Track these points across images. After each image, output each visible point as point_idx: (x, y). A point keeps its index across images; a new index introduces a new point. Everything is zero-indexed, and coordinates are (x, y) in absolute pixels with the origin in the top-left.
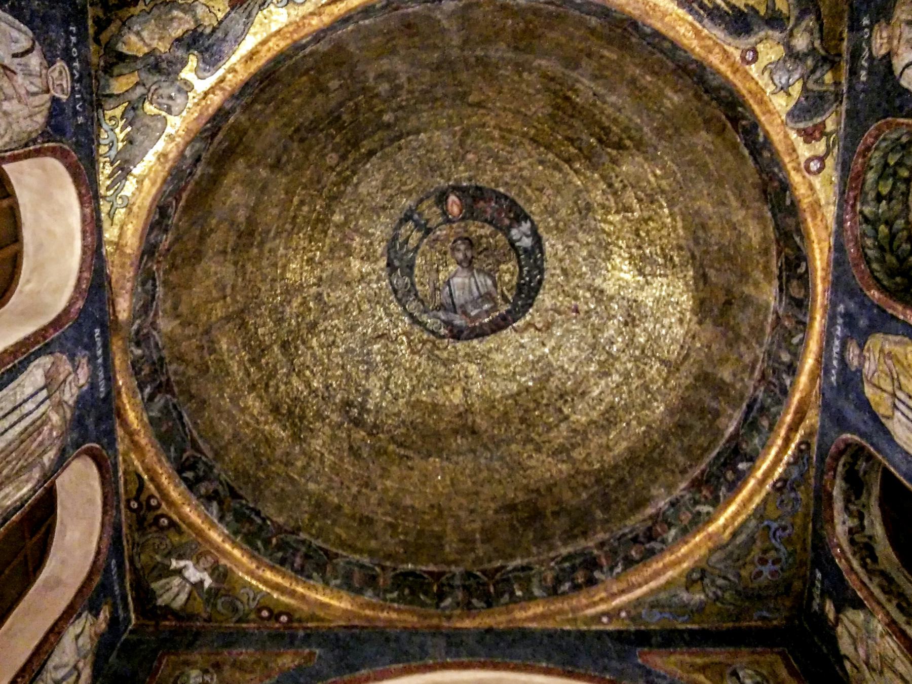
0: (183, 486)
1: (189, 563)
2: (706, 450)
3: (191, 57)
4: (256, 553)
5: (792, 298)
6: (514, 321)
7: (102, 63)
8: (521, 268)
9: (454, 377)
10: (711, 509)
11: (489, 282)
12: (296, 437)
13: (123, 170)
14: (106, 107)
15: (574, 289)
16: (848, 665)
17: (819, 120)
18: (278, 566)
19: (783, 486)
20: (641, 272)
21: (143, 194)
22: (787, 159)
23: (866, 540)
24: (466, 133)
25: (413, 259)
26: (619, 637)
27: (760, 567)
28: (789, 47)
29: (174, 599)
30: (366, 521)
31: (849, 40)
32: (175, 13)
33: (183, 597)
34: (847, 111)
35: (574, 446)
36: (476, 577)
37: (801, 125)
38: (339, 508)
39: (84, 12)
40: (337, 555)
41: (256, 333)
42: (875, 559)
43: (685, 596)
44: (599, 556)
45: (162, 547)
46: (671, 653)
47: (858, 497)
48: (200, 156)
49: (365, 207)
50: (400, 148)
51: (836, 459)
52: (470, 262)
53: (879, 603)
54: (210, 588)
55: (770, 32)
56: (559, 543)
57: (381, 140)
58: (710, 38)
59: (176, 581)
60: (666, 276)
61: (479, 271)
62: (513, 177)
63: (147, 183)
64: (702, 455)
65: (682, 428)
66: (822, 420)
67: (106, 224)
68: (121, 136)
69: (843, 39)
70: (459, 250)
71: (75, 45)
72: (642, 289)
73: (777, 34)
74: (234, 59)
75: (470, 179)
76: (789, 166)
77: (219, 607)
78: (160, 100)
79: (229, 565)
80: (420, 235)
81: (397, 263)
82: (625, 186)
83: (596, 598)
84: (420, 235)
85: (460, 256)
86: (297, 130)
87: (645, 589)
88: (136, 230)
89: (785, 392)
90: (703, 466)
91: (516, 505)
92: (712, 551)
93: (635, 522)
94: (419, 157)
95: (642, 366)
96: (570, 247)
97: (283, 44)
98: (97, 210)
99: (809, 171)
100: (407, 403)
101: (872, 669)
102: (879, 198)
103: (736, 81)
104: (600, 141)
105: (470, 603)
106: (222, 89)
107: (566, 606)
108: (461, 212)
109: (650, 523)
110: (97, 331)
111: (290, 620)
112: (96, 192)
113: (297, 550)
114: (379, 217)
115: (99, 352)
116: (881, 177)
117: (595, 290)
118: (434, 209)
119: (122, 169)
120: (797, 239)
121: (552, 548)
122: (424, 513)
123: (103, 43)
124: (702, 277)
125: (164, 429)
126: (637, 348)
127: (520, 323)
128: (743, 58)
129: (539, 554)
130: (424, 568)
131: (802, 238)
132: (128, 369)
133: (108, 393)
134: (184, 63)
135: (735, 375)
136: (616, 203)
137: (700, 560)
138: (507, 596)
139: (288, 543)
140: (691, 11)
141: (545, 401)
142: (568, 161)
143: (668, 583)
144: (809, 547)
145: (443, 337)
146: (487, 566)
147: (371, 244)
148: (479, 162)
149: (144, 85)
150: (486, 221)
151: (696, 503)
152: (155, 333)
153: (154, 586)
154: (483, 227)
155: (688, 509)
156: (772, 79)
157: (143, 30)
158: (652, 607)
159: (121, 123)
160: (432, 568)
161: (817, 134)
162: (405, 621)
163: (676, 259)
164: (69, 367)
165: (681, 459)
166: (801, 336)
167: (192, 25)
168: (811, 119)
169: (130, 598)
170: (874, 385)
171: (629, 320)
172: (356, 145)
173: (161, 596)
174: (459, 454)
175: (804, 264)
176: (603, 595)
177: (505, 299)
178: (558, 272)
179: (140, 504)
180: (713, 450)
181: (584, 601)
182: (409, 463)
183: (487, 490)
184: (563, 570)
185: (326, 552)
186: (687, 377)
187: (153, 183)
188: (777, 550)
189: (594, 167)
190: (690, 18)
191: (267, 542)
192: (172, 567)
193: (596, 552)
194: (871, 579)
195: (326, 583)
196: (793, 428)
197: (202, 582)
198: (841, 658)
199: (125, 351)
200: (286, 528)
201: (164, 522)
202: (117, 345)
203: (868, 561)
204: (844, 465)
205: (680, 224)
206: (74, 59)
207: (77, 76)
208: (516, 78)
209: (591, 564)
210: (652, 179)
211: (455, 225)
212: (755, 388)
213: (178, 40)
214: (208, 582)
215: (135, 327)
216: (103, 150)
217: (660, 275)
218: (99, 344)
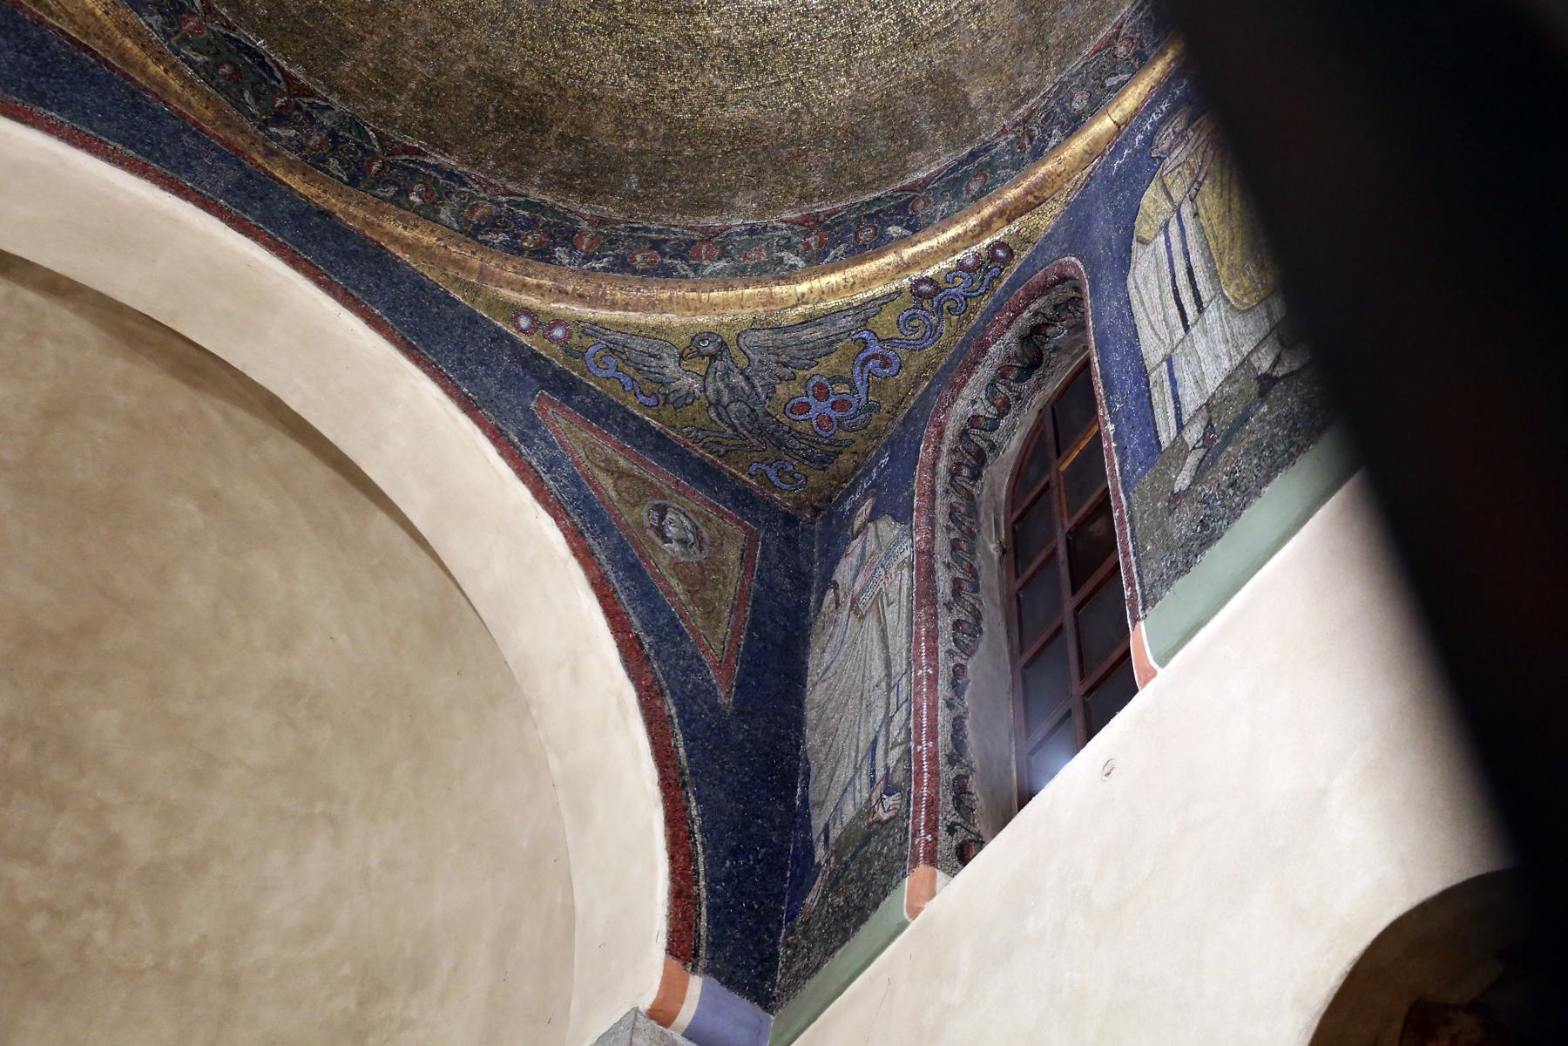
2: (861, 185)
10: (801, 264)
16: (830, 595)
19: (926, 293)
23: (985, 445)
26: (530, 360)
27: (811, 400)
35: (668, 64)
36: (362, 133)
42: (976, 476)
43: (671, 367)
44: (582, 234)
46: (589, 427)
47: (1019, 380)
51: (1031, 298)
53: (932, 522)
56: (537, 180)
64: (850, 189)
65: (855, 138)
66: (1058, 225)
83: (532, 281)
87: (617, 315)
89: (1038, 154)
91: (511, 85)
92: (756, 325)
93: (681, 224)
101: (854, 608)
105: (325, 161)
107: (476, 262)
109: (696, 236)
121: (520, 177)
129: (493, 173)
130: (284, 63)
135: (989, 98)
137: (730, 326)
138: (392, 190)
144: (901, 417)
146: (394, 134)
151: (788, 246)
155: (768, 247)
160: (297, 72)
162: (189, 105)
165: (818, 179)
166: (1126, 76)
170: (1164, 185)
176: (547, 282)
180: (873, 190)
181: (510, 273)
183: (479, 34)
184: (514, 218)
188: (853, 387)
193: (584, 225)
194: (947, 492)
196: (1008, 214)
198: (828, 582)
203: (965, 472)
204: (1036, 314)
212: (1004, 131)
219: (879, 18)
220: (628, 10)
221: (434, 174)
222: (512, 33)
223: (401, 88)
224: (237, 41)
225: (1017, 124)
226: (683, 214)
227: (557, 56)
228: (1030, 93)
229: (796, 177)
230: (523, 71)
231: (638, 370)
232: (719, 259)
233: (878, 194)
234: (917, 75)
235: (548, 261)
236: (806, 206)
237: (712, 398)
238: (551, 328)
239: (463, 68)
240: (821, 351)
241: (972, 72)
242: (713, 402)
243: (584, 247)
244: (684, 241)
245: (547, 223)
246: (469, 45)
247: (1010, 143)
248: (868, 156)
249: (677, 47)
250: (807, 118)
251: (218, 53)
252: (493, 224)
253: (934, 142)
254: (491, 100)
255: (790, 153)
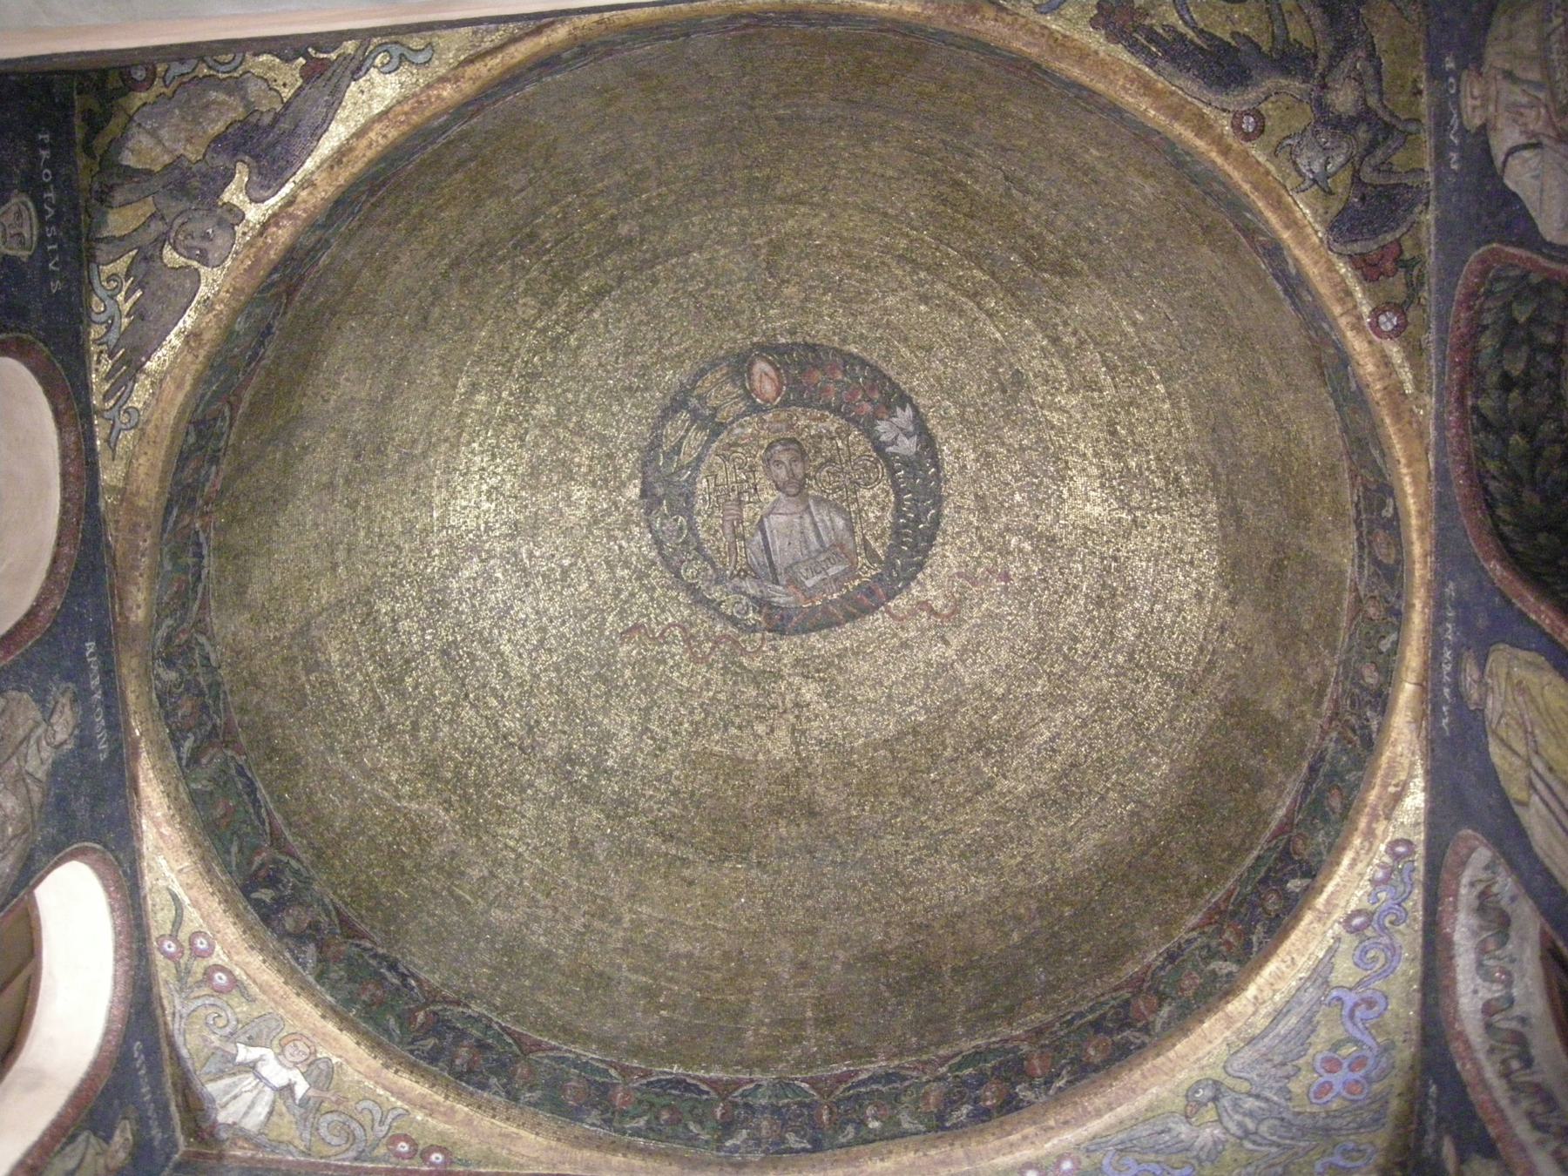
0: (253, 916)
1: (268, 1053)
2: (1237, 852)
3: (239, 166)
4: (384, 1039)
5: (1377, 563)
6: (889, 599)
7: (96, 186)
8: (898, 492)
9: (774, 707)
10: (1234, 968)
11: (840, 523)
12: (471, 827)
13: (130, 365)
14: (100, 259)
15: (1001, 535)
17: (1389, 238)
18: (423, 1064)
20: (1124, 503)
21: (161, 405)
22: (1337, 310)
24: (777, 248)
25: (692, 481)
28: (1321, 106)
29: (246, 1114)
30: (598, 982)
31: (1431, 94)
32: (213, 95)
33: (262, 1110)
34: (1437, 220)
35: (1000, 844)
36: (798, 1091)
37: (1357, 248)
38: (546, 956)
39: (67, 106)
40: (538, 1044)
41: (395, 631)
43: (1183, 1130)
44: (1027, 1057)
45: (221, 1023)
48: (269, 327)
49: (595, 388)
50: (655, 281)
52: (802, 486)
54: (305, 1101)
55: (1283, 82)
56: (960, 1030)
57: (615, 268)
58: (1172, 93)
59: (249, 1081)
60: (1168, 511)
61: (819, 501)
62: (875, 325)
63: (169, 384)
64: (1230, 861)
67: (103, 461)
68: (127, 307)
69: (1420, 92)
70: (779, 463)
71: (48, 164)
72: (1127, 535)
73: (1296, 85)
74: (310, 164)
75: (792, 332)
76: (1343, 322)
77: (323, 1131)
78: (189, 242)
79: (335, 1060)
80: (702, 436)
81: (660, 491)
82: (1082, 342)
84: (702, 436)
85: (782, 474)
86: (455, 264)
88: (153, 466)
90: (1229, 884)
91: (885, 954)
94: (691, 294)
95: (1131, 686)
96: (988, 455)
97: (393, 134)
98: (89, 437)
99: (1379, 333)
100: (684, 757)
102: (1507, 383)
103: (1229, 168)
104: (1028, 260)
105: (783, 1140)
106: (291, 217)
108: (778, 394)
109: (1125, 994)
110: (91, 646)
111: (449, 1160)
112: (88, 403)
113: (461, 1035)
114: (622, 404)
115: (95, 682)
116: (1506, 344)
117: (1040, 536)
118: (728, 387)
119: (128, 363)
120: (1376, 453)
122: (710, 968)
123: (98, 152)
124: (1232, 513)
125: (219, 811)
126: (1119, 650)
127: (900, 603)
128: (1237, 127)
130: (701, 1073)
131: (1383, 455)
132: (151, 706)
133: (116, 752)
134: (228, 177)
135: (1290, 706)
136: (1068, 372)
139: (445, 1022)
140: (1133, 47)
141: (949, 753)
142: (974, 296)
143: (1150, 1108)
145: (754, 629)
147: (610, 456)
148: (807, 299)
149: (163, 218)
150: (827, 406)
151: (1213, 955)
152: (202, 639)
153: (212, 1088)
154: (822, 419)
156: (1294, 163)
157: (161, 126)
158: (1122, 1150)
159: (127, 285)
160: (715, 1074)
161: (1389, 265)
163: (1185, 479)
164: (35, 713)
165: (1194, 869)
166: (1393, 637)
167: (239, 113)
168: (1375, 233)
169: (173, 1108)
171: (1105, 594)
172: (569, 281)
173: (224, 1106)
174: (782, 854)
175: (1390, 501)
177: (872, 555)
178: (970, 502)
179: (179, 945)
182: (686, 873)
185: (518, 1039)
186: (1209, 707)
187: (179, 387)
189: (1023, 308)
190: (1134, 62)
191: (405, 1019)
192: (239, 1059)
193: (1025, 1048)
195: (513, 1096)
197: (290, 1088)
199: (146, 674)
200: (446, 992)
201: (220, 979)
202: (129, 666)
205: (1187, 415)
206: (45, 187)
207: (51, 212)
208: (858, 150)
209: (1014, 1069)
210: (1131, 330)
211: (768, 417)
212: (1324, 733)
213: (219, 138)
214: (301, 1088)
215: (163, 632)
216: (95, 332)
217: (1158, 510)
218: (95, 668)
219: (1146, 688)
220: (938, 820)
221: (874, 1087)
222: (858, 907)
223: (802, 1023)
224: (659, 1081)
225: (1331, 720)
226: (1101, 977)
227: (906, 901)
228: (1322, 685)
229: (1174, 877)
230: (886, 934)
231: (1157, 1152)
232: (1160, 1006)
233: (1255, 853)
234: (1213, 716)
235: (1018, 1108)
236: (1201, 902)
237: (1239, 1133)
238: (1058, 1165)
239: (838, 967)
240: (1304, 1034)
241: (1258, 690)
242: (1239, 1133)
243: (1039, 1072)
244: (1120, 1006)
245: (994, 1068)
246: (831, 944)
247: (1337, 741)
248: (1223, 818)
249: (998, 823)
250: (1147, 814)
251: (652, 1105)
252: (950, 1102)
253: (1272, 773)
254: (877, 980)
255: (1154, 856)
